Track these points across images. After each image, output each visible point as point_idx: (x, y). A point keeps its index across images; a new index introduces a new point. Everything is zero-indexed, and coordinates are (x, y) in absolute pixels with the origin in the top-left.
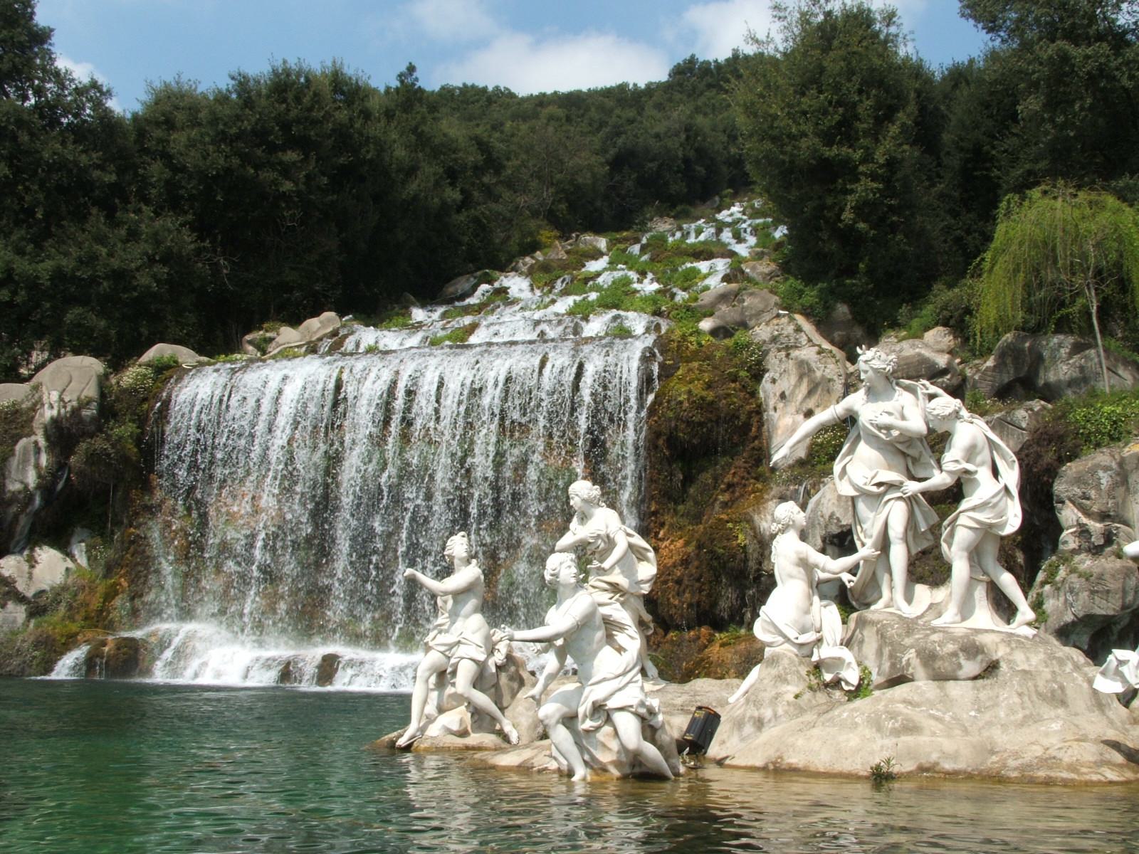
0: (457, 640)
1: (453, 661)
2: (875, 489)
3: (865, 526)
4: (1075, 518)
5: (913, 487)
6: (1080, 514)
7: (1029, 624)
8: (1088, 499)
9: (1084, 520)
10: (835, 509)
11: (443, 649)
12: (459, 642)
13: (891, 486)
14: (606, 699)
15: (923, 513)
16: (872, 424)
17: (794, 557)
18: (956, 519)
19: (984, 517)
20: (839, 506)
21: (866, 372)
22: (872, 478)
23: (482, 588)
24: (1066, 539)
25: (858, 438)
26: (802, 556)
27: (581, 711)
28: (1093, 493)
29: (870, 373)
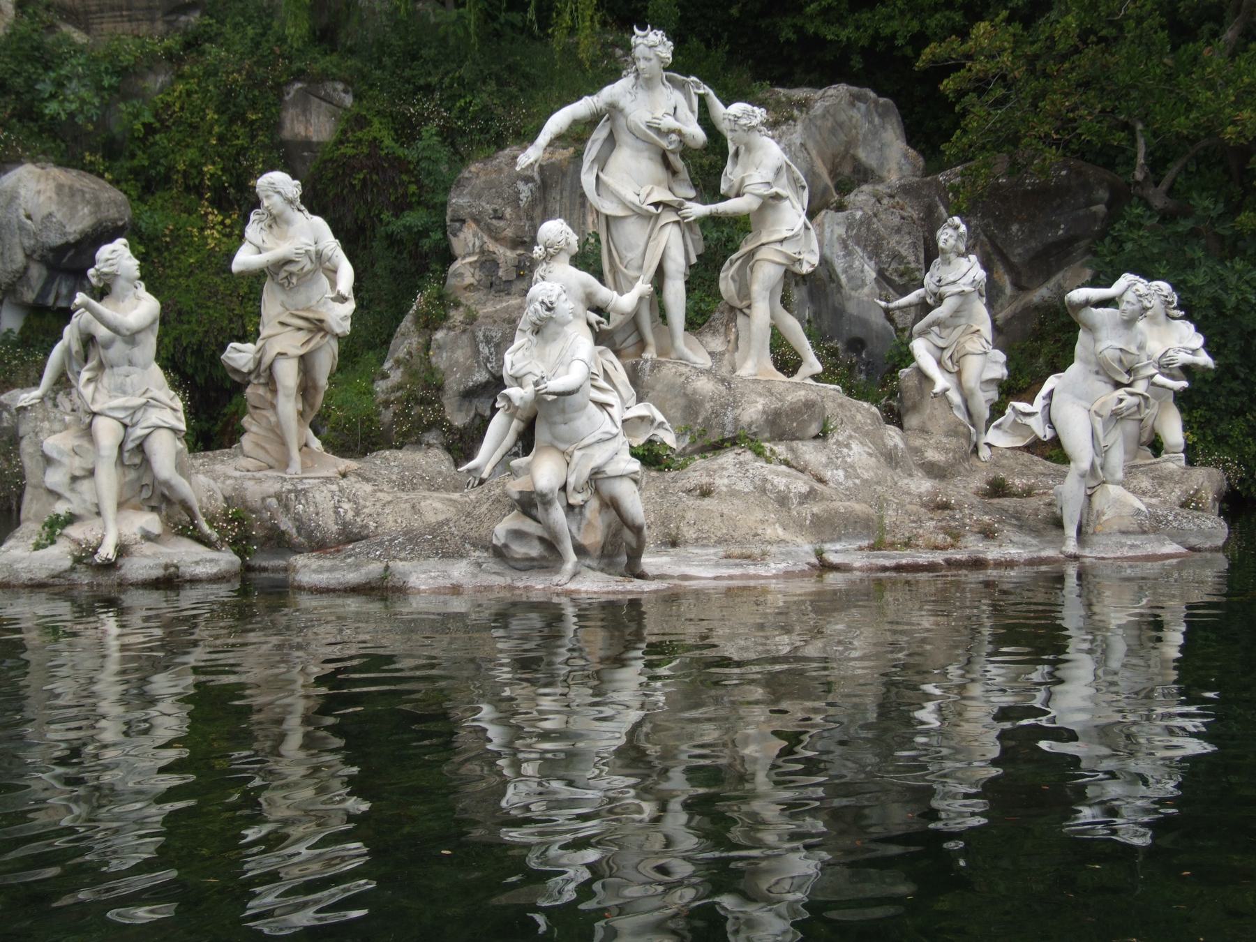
0: (143, 400)
1: (139, 432)
2: (652, 209)
3: (630, 255)
4: (478, 243)
5: (697, 210)
6: (486, 239)
7: (816, 378)
8: (500, 218)
9: (492, 246)
10: (53, 208)
11: (121, 415)
12: (146, 404)
13: (665, 205)
14: (606, 463)
15: (693, 240)
16: (649, 127)
17: (580, 293)
18: (752, 253)
19: (789, 249)
20: (60, 203)
21: (647, 59)
22: (648, 195)
23: (157, 326)
24: (462, 270)
25: (611, 142)
26: (588, 290)
27: (572, 480)
28: (508, 212)
29: (655, 62)
